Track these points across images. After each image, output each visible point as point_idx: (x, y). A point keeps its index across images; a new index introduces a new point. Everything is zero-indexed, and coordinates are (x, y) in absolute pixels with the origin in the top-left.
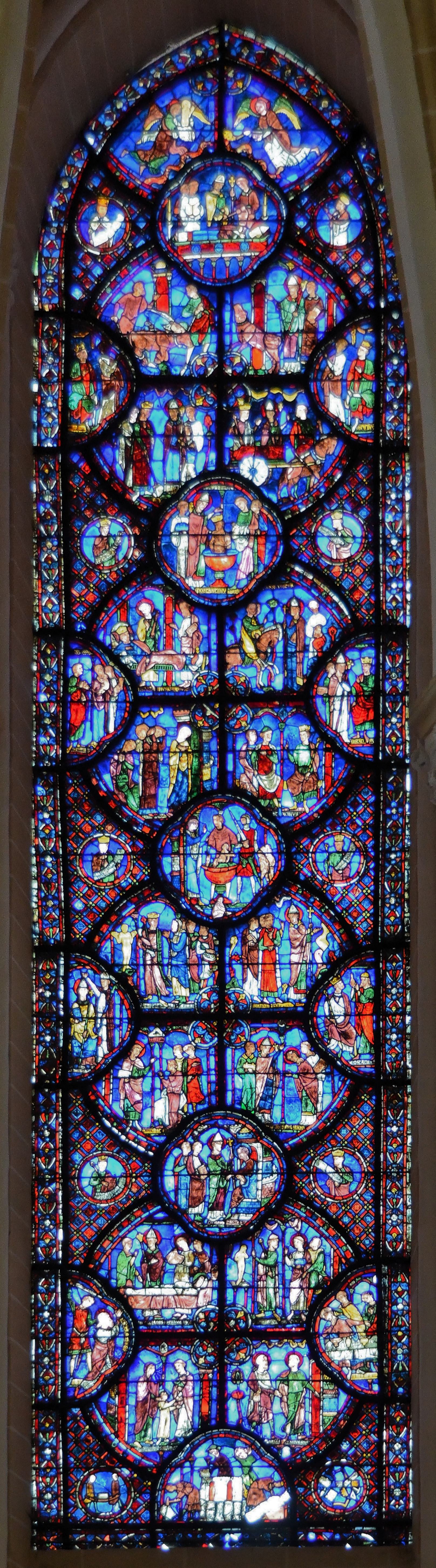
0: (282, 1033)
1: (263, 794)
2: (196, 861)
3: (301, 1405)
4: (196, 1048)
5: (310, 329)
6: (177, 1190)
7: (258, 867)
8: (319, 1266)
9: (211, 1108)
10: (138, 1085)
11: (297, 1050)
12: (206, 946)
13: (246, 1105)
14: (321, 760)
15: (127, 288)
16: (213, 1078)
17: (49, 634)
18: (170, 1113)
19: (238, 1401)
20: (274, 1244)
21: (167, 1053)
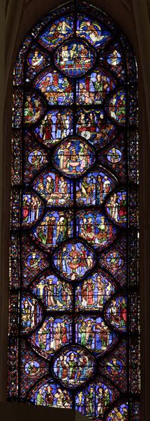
0: (95, 319)
4: (65, 324)
5: (104, 91)
6: (58, 372)
9: (70, 344)
10: (44, 336)
11: (100, 324)
15: (44, 78)
20: (92, 391)
21: (55, 326)
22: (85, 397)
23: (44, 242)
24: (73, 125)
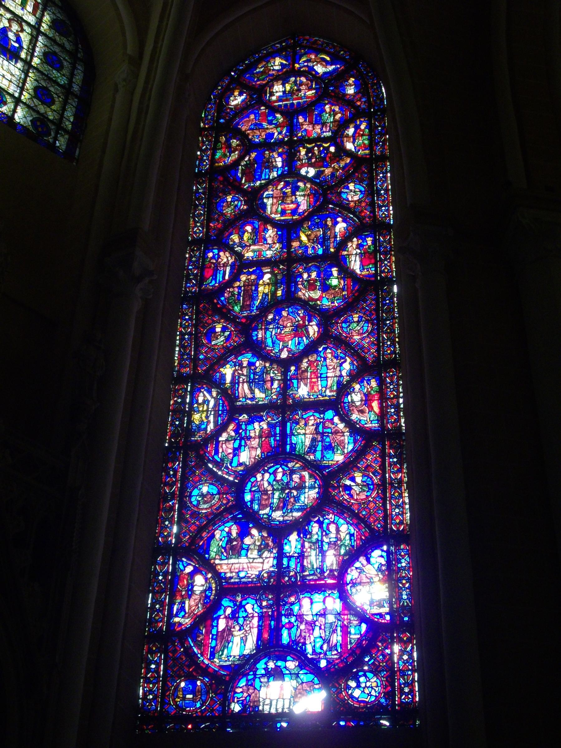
2: (272, 332)
3: (334, 631)
6: (252, 501)
7: (308, 332)
12: (276, 372)
13: (299, 452)
14: (344, 282)
16: (278, 438)
18: (250, 458)
19: (289, 629)
21: (250, 427)
23: (237, 309)
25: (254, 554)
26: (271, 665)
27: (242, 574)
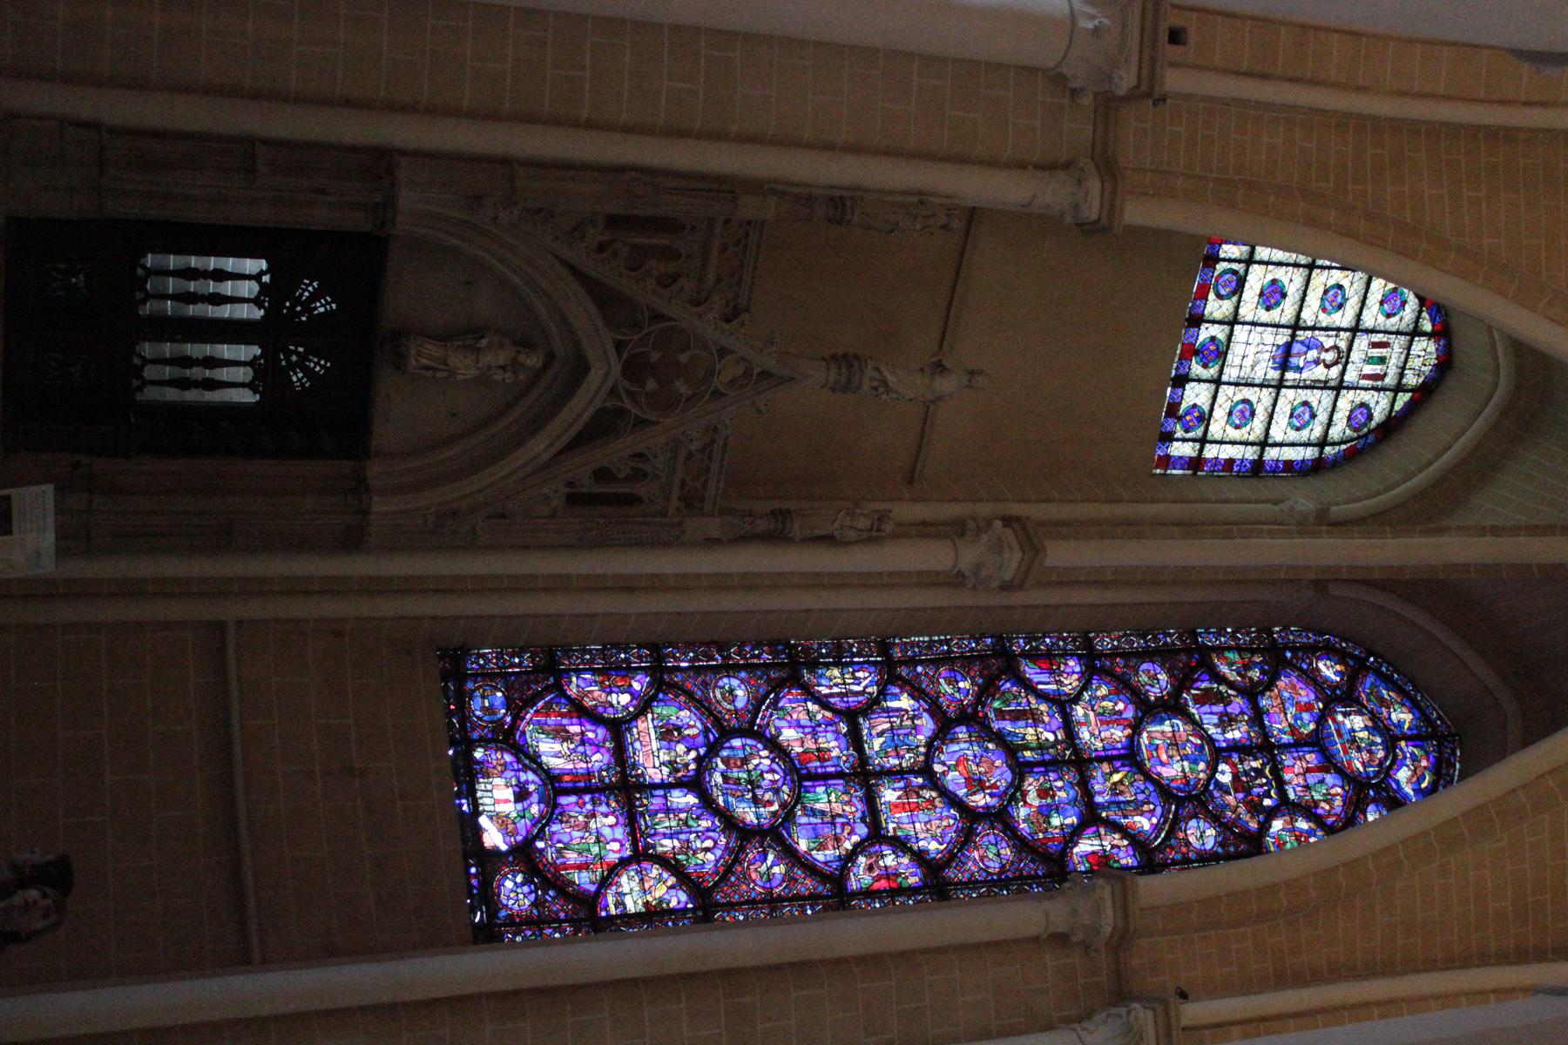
0: (863, 819)
1: (1024, 794)
3: (580, 854)
5: (1316, 803)
6: (732, 748)
8: (693, 861)
9: (797, 770)
11: (852, 832)
17: (1088, 644)
22: (688, 810)
23: (996, 704)
24: (1234, 747)
25: (664, 757)
26: (532, 788)
27: (637, 745)
